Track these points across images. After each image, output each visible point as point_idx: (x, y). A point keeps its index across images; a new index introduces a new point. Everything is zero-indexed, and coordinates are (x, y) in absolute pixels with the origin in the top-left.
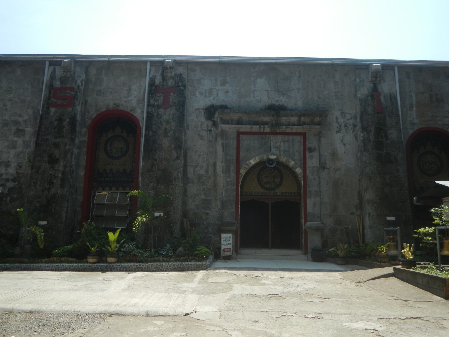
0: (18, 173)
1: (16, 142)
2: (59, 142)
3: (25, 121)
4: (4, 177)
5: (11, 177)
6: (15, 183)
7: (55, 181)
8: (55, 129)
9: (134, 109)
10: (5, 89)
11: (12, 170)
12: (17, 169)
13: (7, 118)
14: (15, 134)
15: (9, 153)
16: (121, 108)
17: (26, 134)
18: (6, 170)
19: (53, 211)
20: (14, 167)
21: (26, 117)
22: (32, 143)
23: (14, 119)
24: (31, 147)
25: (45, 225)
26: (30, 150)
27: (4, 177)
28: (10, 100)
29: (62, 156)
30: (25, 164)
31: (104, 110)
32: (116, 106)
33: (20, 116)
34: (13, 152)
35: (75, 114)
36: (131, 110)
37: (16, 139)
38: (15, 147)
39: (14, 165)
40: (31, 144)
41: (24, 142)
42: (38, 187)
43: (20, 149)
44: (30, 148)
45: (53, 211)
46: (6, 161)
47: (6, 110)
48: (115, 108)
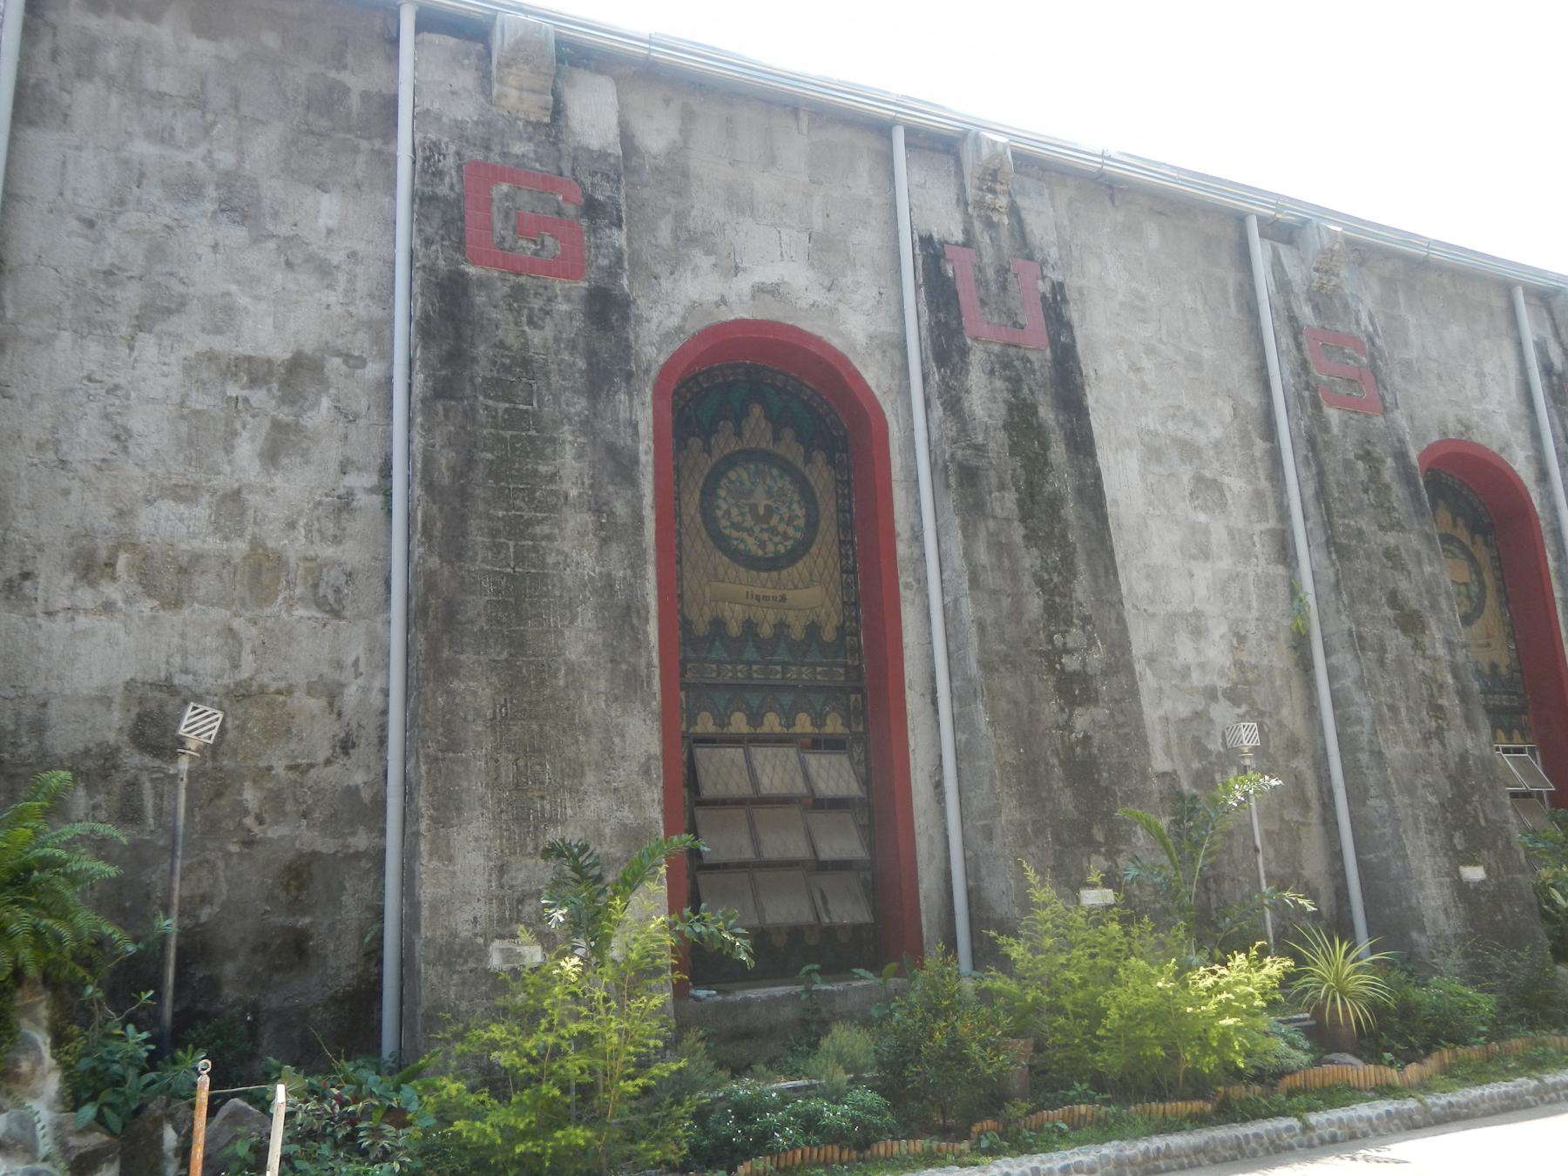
0: (1239, 665)
1: (1206, 531)
2: (1397, 548)
3: (1216, 445)
4: (1196, 678)
5: (1223, 684)
6: (1239, 707)
7: (1444, 702)
8: (1366, 491)
9: (1506, 446)
10: (1121, 297)
11: (1217, 652)
12: (1233, 649)
13: (1151, 422)
14: (1191, 494)
15: (1191, 575)
16: (1477, 438)
17: (1230, 502)
18: (1198, 651)
19: (1483, 822)
20: (1222, 637)
21: (1217, 433)
22: (1256, 538)
23: (1180, 434)
24: (1257, 557)
25: (1483, 882)
26: (1259, 570)
27: (1196, 678)
28: (1150, 351)
29: (1426, 603)
30: (1252, 628)
31: (1435, 437)
32: (1463, 429)
33: (1198, 423)
34: (1204, 573)
35: (1400, 441)
36: (1502, 450)
37: (1202, 517)
38: (1205, 554)
39: (1218, 629)
40: (1254, 545)
41: (1231, 533)
42: (1407, 726)
43: (1225, 563)
44: (1254, 560)
45: (1483, 822)
46: (1189, 610)
47: (1144, 388)
48: (1462, 434)
